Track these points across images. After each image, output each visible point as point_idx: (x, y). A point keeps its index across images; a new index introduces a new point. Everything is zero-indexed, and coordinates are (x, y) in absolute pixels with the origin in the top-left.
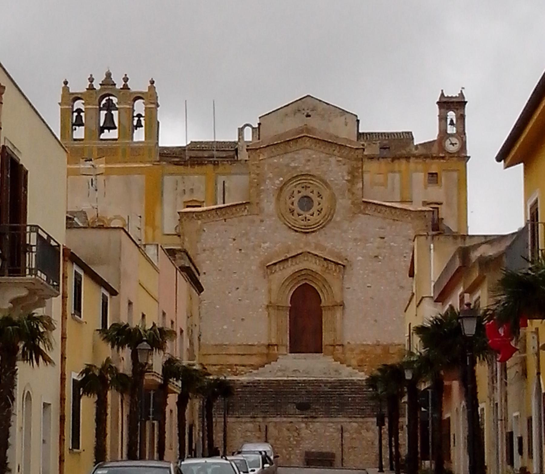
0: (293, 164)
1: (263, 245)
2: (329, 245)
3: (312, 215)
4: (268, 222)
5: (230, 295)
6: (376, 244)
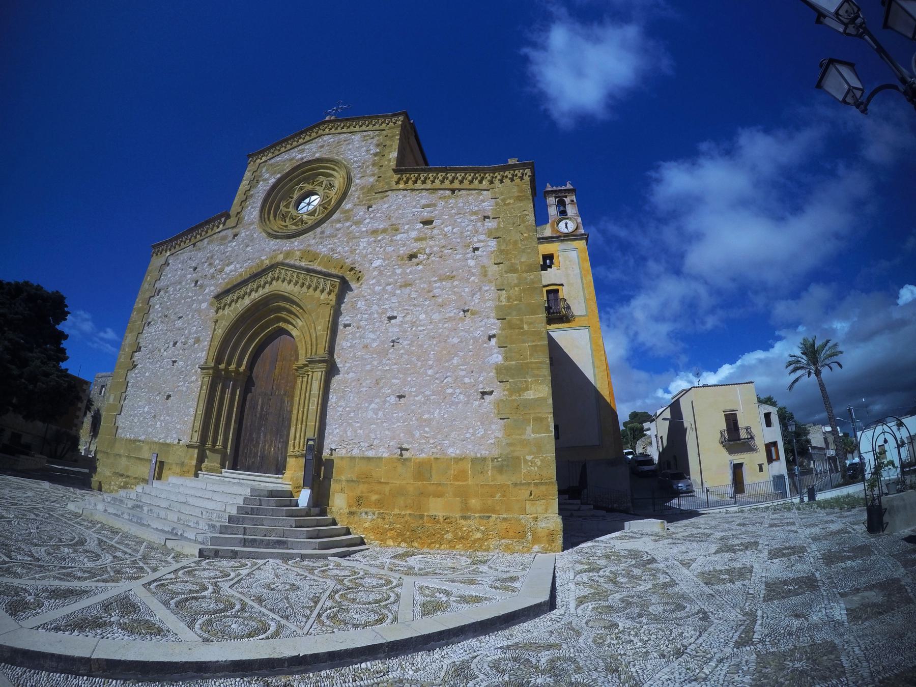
2: (323, 250)
6: (414, 234)
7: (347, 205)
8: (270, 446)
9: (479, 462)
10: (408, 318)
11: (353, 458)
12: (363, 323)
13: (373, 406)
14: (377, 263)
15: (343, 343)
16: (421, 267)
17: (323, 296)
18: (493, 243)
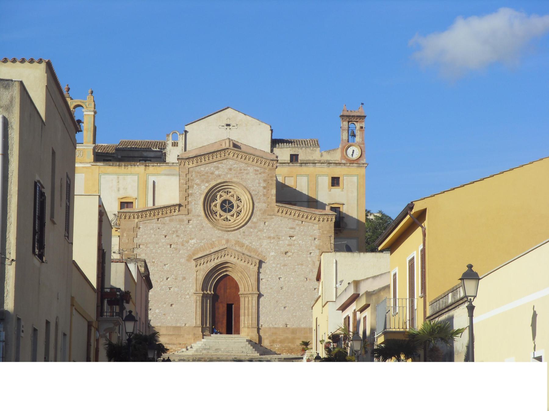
0: (217, 173)
1: (190, 241)
3: (233, 216)
4: (194, 222)
6: (287, 242)
7: (254, 219)
11: (270, 328)
12: (269, 279)
14: (273, 254)
15: (262, 287)
16: (290, 258)
17: (252, 267)
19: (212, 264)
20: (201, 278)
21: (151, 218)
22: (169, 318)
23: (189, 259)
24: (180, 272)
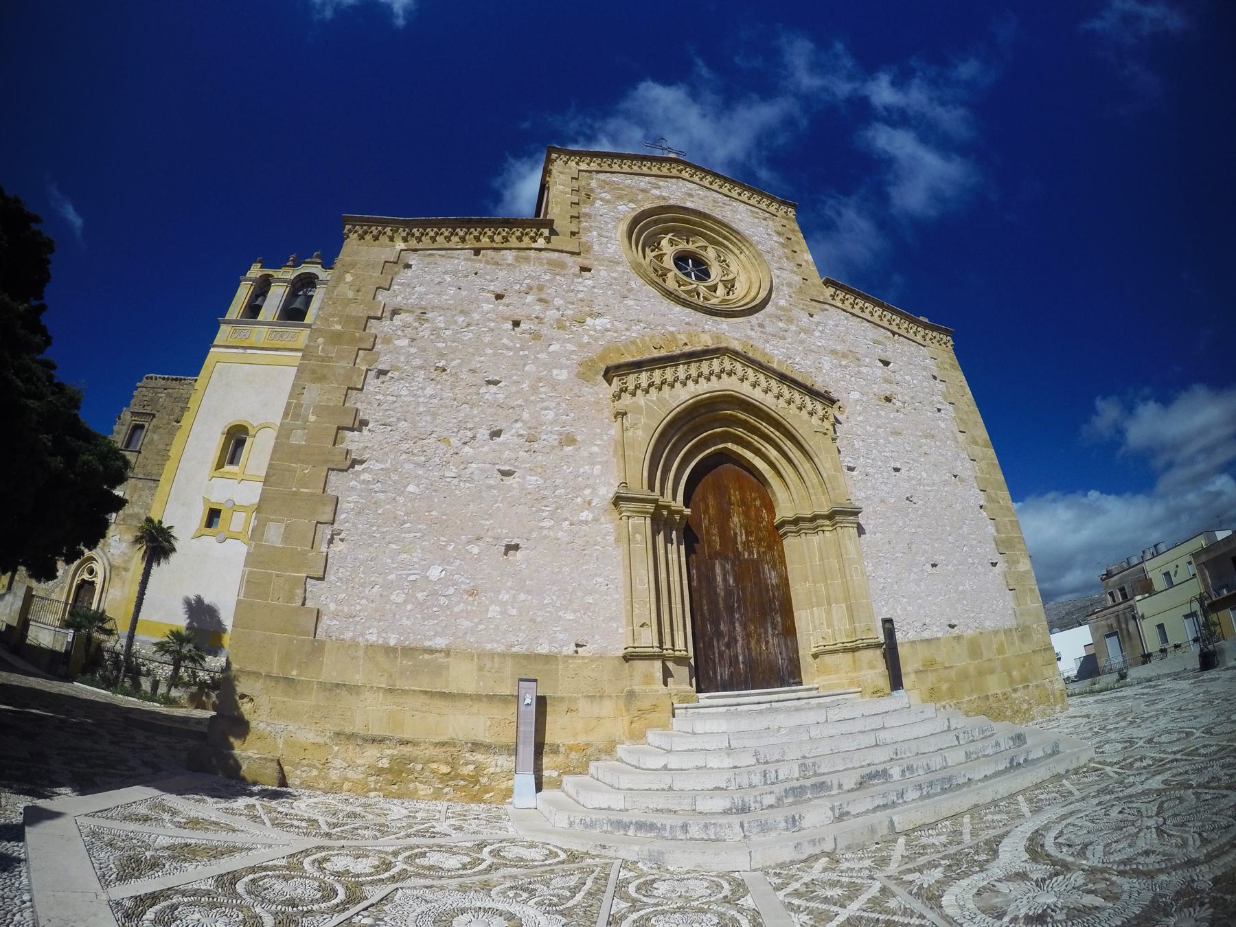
0: (657, 192)
1: (589, 321)
3: (714, 289)
4: (602, 272)
5: (467, 449)
8: (758, 641)
9: (1008, 632)
10: (912, 473)
12: (869, 470)
13: (913, 576)
14: (855, 395)
17: (815, 420)
18: (950, 408)
19: (683, 395)
20: (643, 434)
21: (451, 245)
22: (494, 611)
23: (585, 372)
24: (551, 415)
